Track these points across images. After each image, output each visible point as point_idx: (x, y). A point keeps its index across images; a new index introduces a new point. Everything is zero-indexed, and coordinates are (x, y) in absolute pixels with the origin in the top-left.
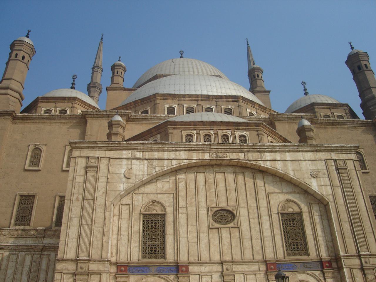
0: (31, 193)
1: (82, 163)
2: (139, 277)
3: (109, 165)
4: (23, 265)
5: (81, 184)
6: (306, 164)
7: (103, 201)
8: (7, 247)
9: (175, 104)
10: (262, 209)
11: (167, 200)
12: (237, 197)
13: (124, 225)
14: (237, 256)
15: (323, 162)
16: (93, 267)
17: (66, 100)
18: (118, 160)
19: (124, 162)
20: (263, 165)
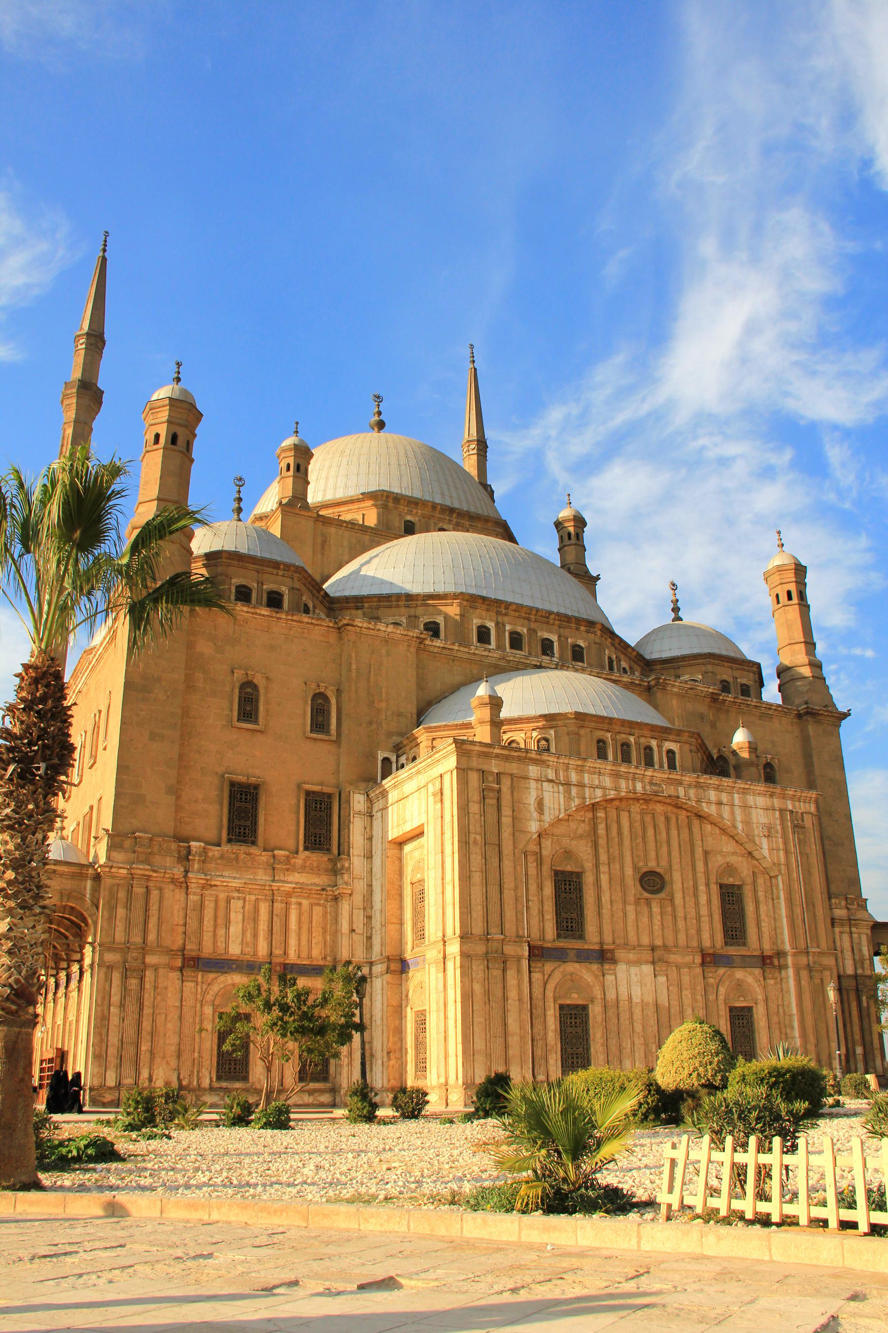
0: (253, 780)
1: (474, 778)
2: (557, 964)
3: (512, 788)
4: (256, 920)
5: (477, 817)
6: (757, 814)
7: (511, 848)
8: (225, 884)
9: (491, 620)
10: (699, 875)
11: (583, 850)
12: (669, 853)
13: (533, 888)
14: (670, 942)
15: (777, 813)
16: (509, 949)
17: (279, 568)
18: (523, 781)
19: (533, 784)
20: (706, 810)
